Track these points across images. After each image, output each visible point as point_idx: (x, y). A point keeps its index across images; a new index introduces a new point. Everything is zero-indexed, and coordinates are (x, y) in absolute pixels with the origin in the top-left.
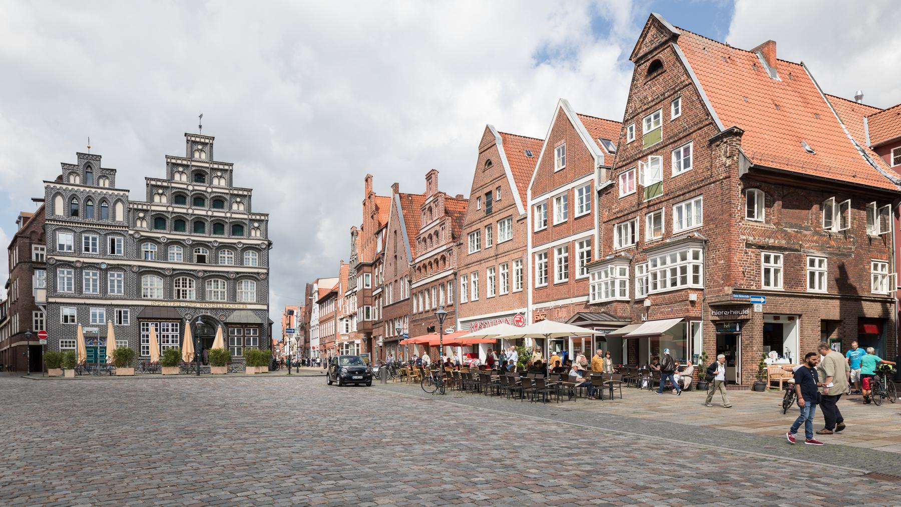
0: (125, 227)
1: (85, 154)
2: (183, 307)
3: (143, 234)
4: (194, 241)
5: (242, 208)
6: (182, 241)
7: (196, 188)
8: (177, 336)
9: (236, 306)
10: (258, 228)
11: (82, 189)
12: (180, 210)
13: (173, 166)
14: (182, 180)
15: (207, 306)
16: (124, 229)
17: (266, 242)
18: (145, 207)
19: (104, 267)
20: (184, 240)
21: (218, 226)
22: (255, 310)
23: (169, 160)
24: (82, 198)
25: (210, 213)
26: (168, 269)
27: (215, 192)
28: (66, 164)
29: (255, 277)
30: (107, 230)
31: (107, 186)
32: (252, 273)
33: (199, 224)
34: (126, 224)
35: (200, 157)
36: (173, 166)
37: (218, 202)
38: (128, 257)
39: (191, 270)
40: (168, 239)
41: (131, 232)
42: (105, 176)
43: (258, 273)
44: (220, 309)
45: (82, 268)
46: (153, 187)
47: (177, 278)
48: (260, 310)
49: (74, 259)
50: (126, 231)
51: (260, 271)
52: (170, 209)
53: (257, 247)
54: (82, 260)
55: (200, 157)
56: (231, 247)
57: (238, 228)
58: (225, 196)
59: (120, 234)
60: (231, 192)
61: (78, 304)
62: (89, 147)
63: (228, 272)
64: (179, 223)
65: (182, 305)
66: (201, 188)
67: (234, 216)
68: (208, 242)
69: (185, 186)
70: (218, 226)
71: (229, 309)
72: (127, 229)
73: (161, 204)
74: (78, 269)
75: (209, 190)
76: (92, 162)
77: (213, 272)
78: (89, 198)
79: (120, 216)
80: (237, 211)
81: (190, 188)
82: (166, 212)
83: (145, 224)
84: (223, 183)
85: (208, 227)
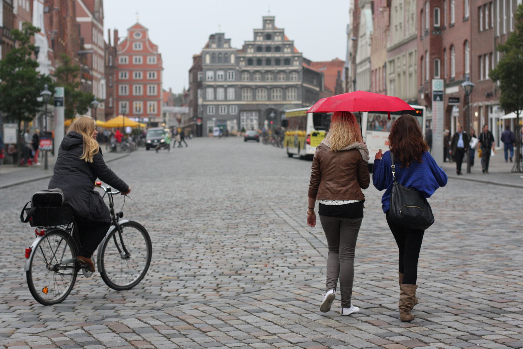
12: (259, 55)
19: (226, 86)
21: (278, 61)
24: (217, 54)
33: (268, 61)
37: (278, 49)
38: (237, 80)
43: (297, 85)
56: (283, 71)
57: (287, 61)
64: (259, 61)
66: (269, 43)
70: (278, 61)
73: (250, 53)
74: (215, 88)
80: (287, 53)
84: (280, 38)
85: (273, 62)
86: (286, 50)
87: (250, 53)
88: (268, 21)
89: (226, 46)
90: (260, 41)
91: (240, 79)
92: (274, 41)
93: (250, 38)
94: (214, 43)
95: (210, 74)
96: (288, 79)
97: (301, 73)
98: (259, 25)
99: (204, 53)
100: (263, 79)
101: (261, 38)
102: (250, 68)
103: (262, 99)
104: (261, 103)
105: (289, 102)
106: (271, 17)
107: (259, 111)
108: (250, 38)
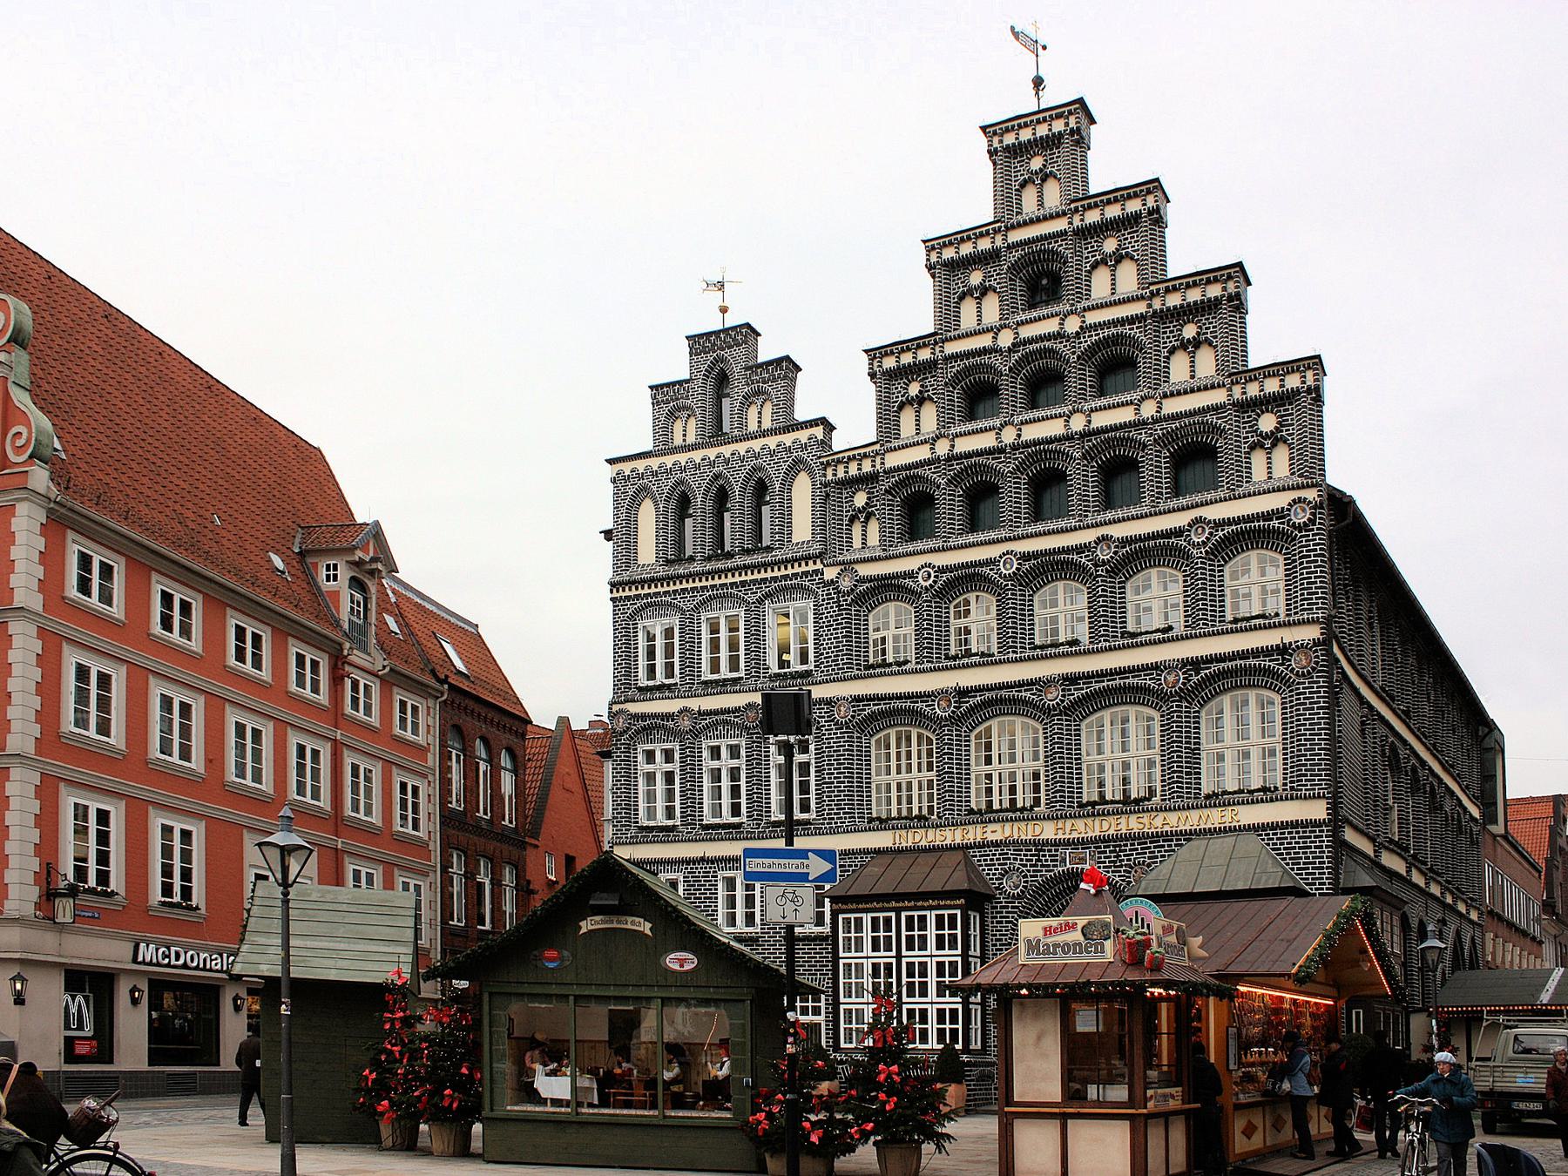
0: (814, 558)
1: (717, 333)
2: (996, 844)
3: (865, 570)
4: (1026, 557)
6: (986, 570)
7: (1027, 332)
9: (1193, 820)
16: (811, 567)
17: (1311, 495)
18: (867, 467)
20: (991, 562)
22: (1273, 826)
23: (934, 258)
26: (943, 693)
27: (1096, 327)
28: (662, 386)
29: (1268, 672)
30: (764, 580)
32: (1255, 653)
34: (816, 548)
35: (1041, 204)
39: (1020, 685)
41: (830, 574)
42: (758, 393)
43: (1283, 650)
44: (1130, 837)
45: (696, 734)
47: (981, 728)
48: (1294, 825)
50: (816, 572)
52: (942, 448)
53: (1275, 523)
55: (1041, 204)
58: (1134, 331)
59: (801, 588)
60: (1157, 304)
61: (688, 861)
62: (724, 310)
63: (1156, 666)
65: (991, 837)
67: (1173, 406)
68: (1080, 549)
71: (1167, 836)
72: (819, 566)
75: (1072, 325)
76: (726, 353)
77: (1101, 675)
81: (1006, 339)
82: (928, 462)
86: (1179, 368)
89: (760, 416)
102: (916, 562)
104: (996, 832)
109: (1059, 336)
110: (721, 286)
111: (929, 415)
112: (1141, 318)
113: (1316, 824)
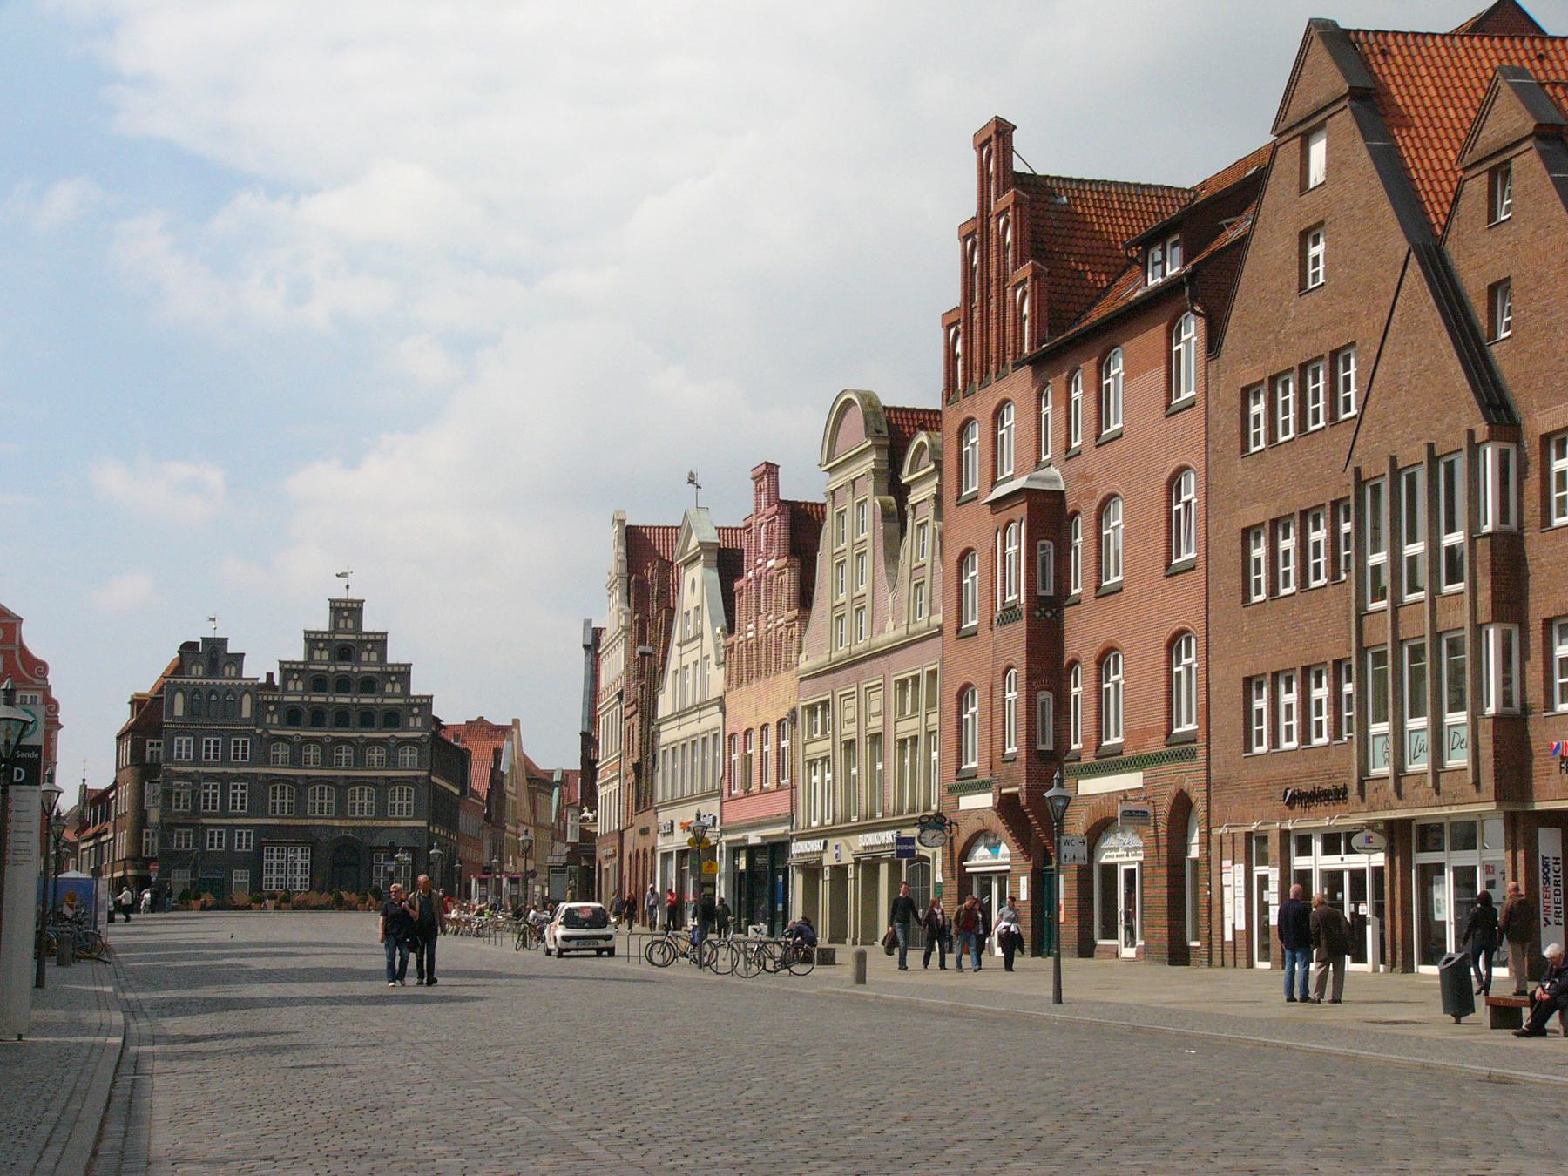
2: (318, 826)
3: (272, 732)
5: (398, 688)
7: (339, 668)
8: (307, 865)
9: (385, 823)
10: (418, 715)
11: (205, 682)
13: (312, 640)
14: (323, 662)
15: (348, 823)
21: (367, 718)
25: (355, 700)
31: (233, 674)
33: (342, 717)
36: (312, 640)
37: (368, 685)
40: (303, 737)
41: (259, 731)
43: (416, 778)
46: (287, 669)
49: (192, 770)
51: (419, 773)
52: (306, 698)
54: (201, 770)
56: (381, 742)
57: (393, 718)
64: (318, 716)
67: (387, 701)
69: (325, 668)
70: (367, 718)
75: (355, 670)
77: (358, 777)
78: (212, 692)
79: (246, 712)
81: (332, 669)
83: (275, 719)
84: (374, 656)
86: (388, 688)
87: (295, 693)
88: (346, 611)
90: (321, 662)
91: (266, 764)
92: (359, 663)
93: (297, 653)
94: (196, 662)
95: (183, 743)
96: (392, 763)
97: (428, 747)
98: (322, 623)
99: (165, 690)
100: (326, 762)
101: (325, 656)
103: (321, 816)
104: (318, 822)
105: (392, 823)
106: (352, 602)
107: (314, 845)
108: (297, 653)
109: (351, 672)
110: (214, 620)
111: (300, 686)
112: (378, 673)
113: (423, 828)
